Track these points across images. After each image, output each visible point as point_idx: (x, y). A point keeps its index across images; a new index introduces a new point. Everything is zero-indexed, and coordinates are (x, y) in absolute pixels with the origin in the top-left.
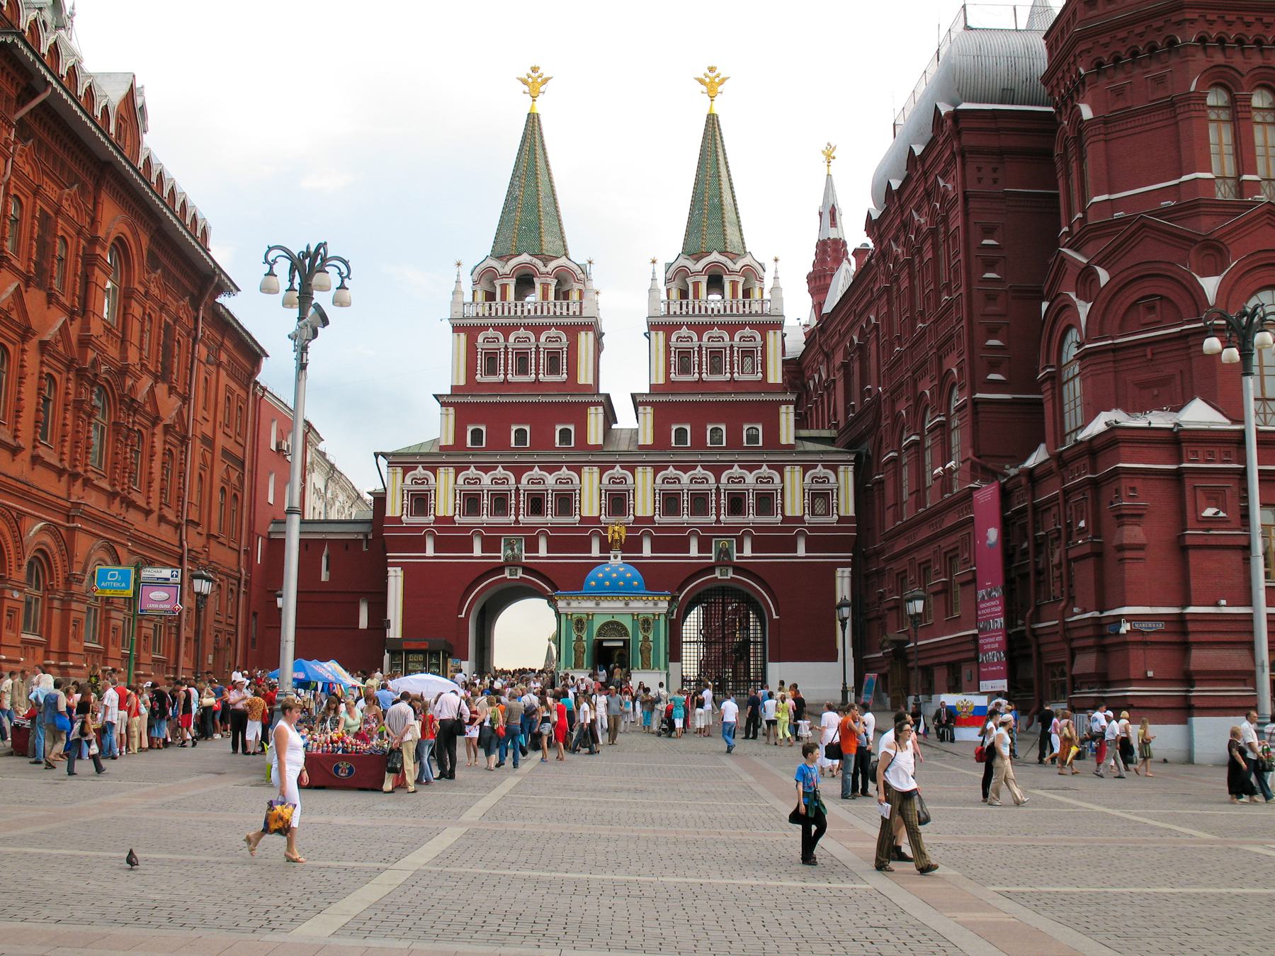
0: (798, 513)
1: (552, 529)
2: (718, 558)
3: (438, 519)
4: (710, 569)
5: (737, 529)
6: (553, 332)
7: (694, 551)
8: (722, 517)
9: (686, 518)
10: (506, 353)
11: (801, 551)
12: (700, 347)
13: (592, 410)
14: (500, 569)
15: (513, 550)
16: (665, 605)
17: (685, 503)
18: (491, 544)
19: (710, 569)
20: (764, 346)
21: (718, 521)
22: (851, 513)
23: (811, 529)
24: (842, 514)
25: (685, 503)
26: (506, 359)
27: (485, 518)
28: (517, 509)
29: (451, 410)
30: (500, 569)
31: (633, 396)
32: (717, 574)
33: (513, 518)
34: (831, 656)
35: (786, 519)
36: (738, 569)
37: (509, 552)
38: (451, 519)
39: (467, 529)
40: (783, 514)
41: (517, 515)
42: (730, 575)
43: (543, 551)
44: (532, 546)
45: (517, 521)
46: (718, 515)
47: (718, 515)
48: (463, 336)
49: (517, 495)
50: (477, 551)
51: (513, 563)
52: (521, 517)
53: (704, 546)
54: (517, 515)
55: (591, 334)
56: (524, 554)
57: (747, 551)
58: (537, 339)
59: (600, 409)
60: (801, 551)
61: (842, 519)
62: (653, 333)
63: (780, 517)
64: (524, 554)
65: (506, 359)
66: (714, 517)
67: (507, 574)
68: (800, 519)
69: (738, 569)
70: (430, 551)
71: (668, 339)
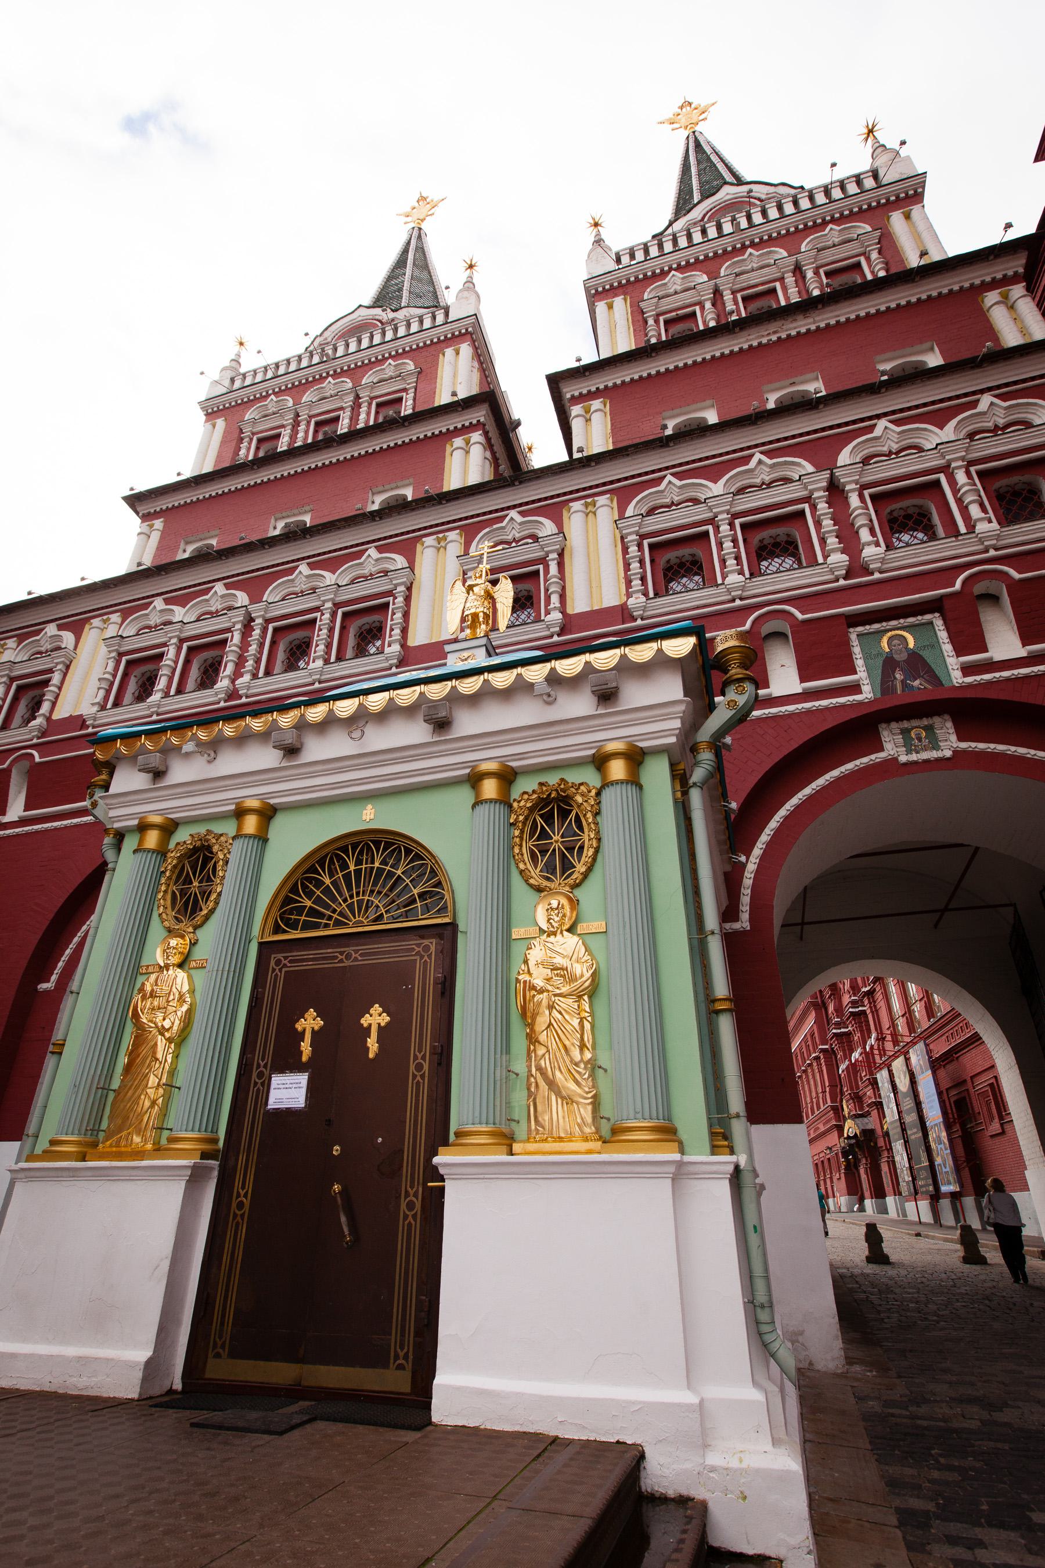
4: (858, 730)
6: (389, 368)
7: (784, 677)
8: (870, 552)
10: (296, 424)
13: (458, 442)
16: (670, 689)
17: (726, 547)
21: (857, 567)
25: (726, 547)
29: (158, 524)
31: (555, 381)
32: (892, 746)
48: (221, 423)
53: (821, 653)
55: (466, 349)
59: (477, 437)
62: (601, 307)
70: (16, 809)
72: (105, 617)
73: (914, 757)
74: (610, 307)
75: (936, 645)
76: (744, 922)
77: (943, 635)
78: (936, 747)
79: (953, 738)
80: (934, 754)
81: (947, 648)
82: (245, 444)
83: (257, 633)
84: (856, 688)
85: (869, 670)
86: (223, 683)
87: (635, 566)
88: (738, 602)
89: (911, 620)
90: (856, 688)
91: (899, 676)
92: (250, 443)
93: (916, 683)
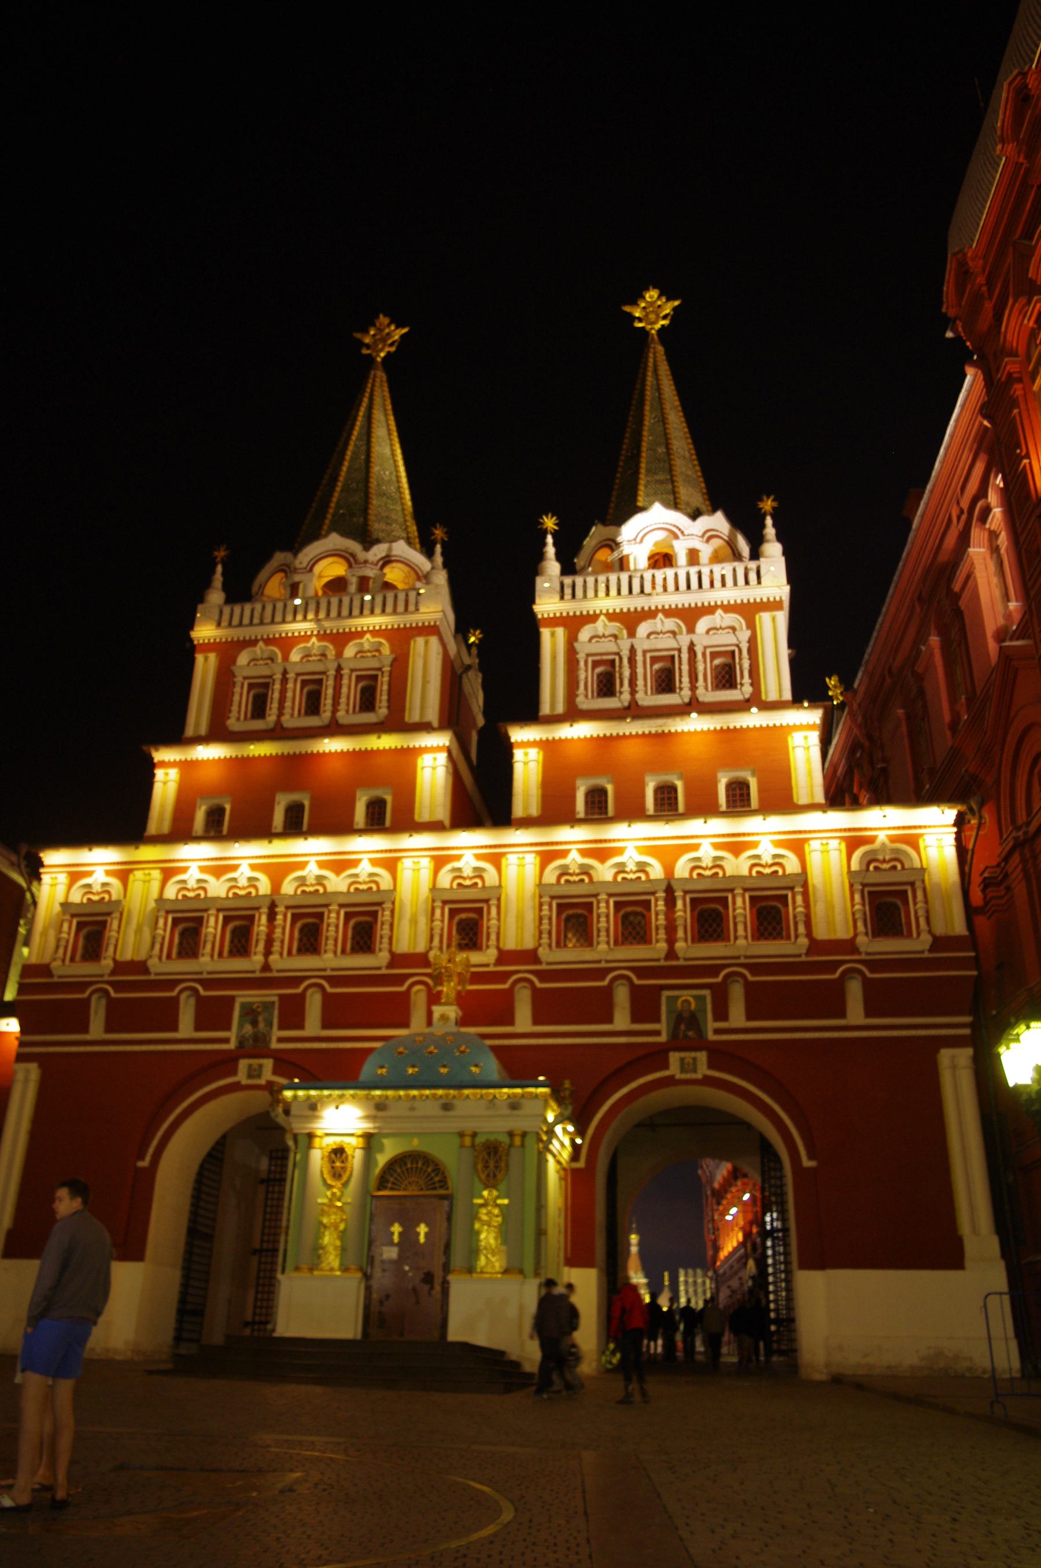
0: (842, 932)
1: (334, 981)
2: (674, 1034)
3: (120, 967)
4: (656, 1057)
5: (713, 970)
7: (621, 1020)
8: (680, 945)
9: (603, 950)
10: (284, 680)
11: (855, 1012)
12: (633, 650)
14: (226, 1063)
15: (255, 1023)
18: (213, 1014)
19: (656, 1057)
20: (753, 641)
21: (671, 954)
22: (959, 927)
23: (874, 965)
24: (939, 930)
26: (283, 692)
27: (207, 963)
28: (269, 942)
30: (226, 1063)
33: (258, 959)
34: (948, 1254)
35: (816, 946)
36: (719, 1055)
37: (248, 1029)
38: (140, 967)
39: (170, 984)
40: (809, 934)
41: (268, 952)
42: (703, 1070)
43: (313, 1025)
44: (292, 1013)
45: (266, 967)
46: (671, 941)
47: (671, 941)
49: (272, 916)
50: (186, 1027)
52: (274, 958)
53: (644, 1006)
54: (268, 952)
55: (434, 640)
56: (276, 1033)
57: (737, 1016)
58: (339, 654)
60: (855, 1012)
61: (939, 943)
63: (803, 941)
64: (276, 1033)
65: (283, 692)
66: (663, 946)
67: (241, 1076)
68: (849, 946)
69: (719, 1055)
70: (96, 1029)
71: (572, 640)
72: (147, 872)
73: (684, 1076)
74: (553, 634)
75: (705, 1011)
76: (581, 1164)
77: (709, 1007)
78: (695, 1071)
79: (705, 1067)
80: (693, 1076)
81: (710, 1015)
82: (237, 689)
83: (280, 917)
84: (658, 1033)
85: (668, 1024)
86: (258, 959)
87: (545, 921)
88: (603, 965)
89: (695, 992)
90: (658, 1033)
91: (683, 1027)
92: (242, 688)
93: (690, 1033)
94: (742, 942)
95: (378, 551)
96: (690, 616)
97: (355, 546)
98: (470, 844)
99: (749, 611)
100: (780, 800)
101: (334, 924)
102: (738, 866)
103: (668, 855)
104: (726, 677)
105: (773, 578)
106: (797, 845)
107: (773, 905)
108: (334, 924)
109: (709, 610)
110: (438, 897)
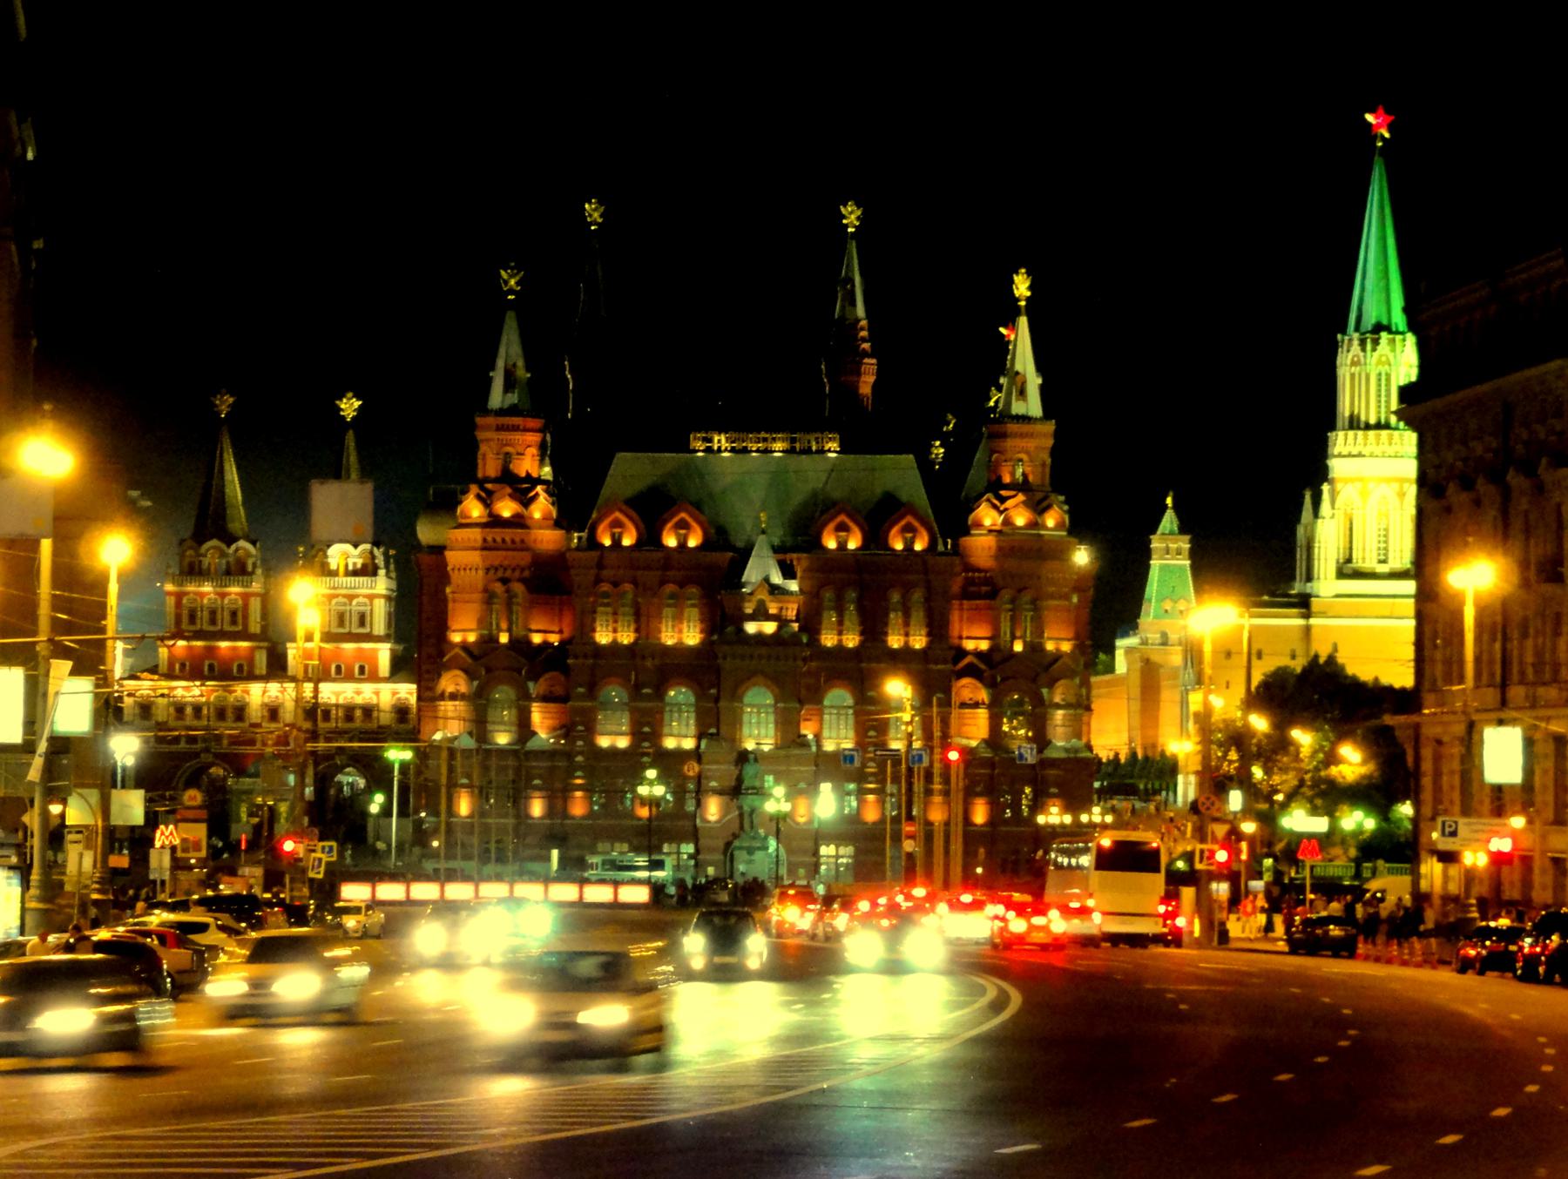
51: (207, 750)
68: (389, 727)
94: (358, 723)
95: (233, 547)
96: (351, 597)
97: (224, 546)
98: (274, 688)
99: (371, 597)
100: (374, 678)
101: (230, 714)
102: (359, 700)
103: (337, 694)
104: (362, 623)
105: (382, 584)
106: (377, 693)
107: (368, 711)
108: (230, 714)
109: (357, 596)
110: (264, 705)
